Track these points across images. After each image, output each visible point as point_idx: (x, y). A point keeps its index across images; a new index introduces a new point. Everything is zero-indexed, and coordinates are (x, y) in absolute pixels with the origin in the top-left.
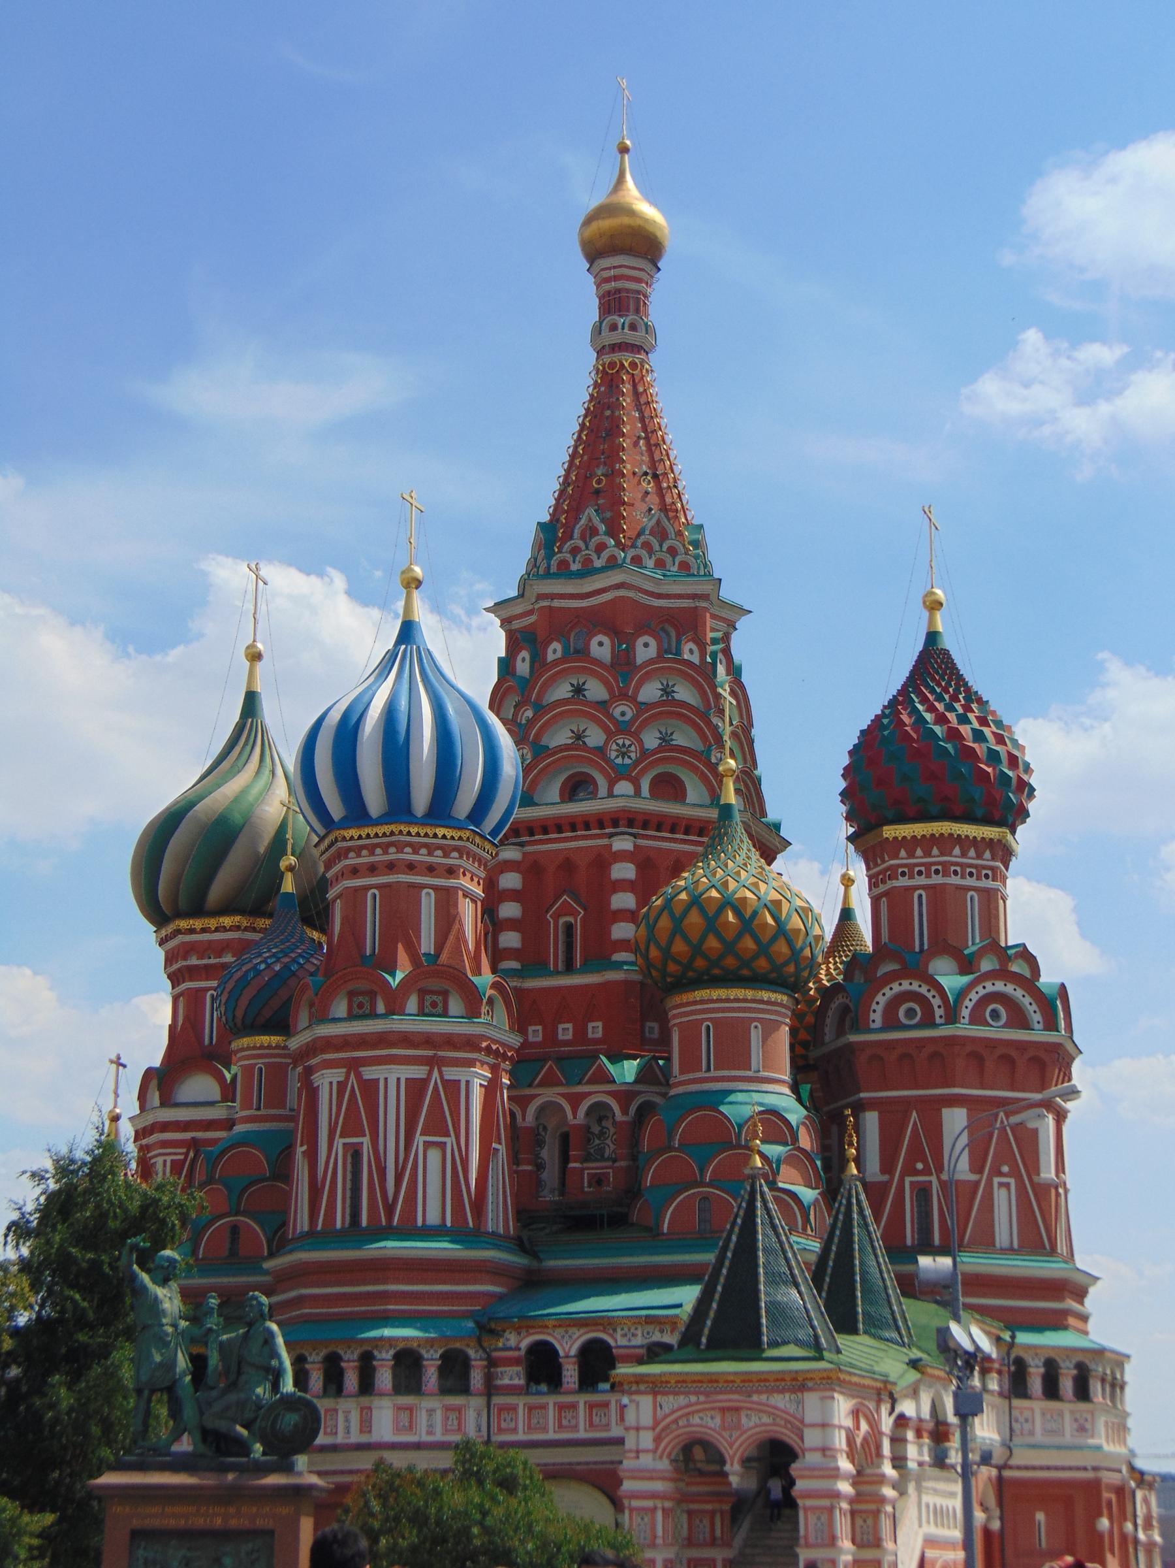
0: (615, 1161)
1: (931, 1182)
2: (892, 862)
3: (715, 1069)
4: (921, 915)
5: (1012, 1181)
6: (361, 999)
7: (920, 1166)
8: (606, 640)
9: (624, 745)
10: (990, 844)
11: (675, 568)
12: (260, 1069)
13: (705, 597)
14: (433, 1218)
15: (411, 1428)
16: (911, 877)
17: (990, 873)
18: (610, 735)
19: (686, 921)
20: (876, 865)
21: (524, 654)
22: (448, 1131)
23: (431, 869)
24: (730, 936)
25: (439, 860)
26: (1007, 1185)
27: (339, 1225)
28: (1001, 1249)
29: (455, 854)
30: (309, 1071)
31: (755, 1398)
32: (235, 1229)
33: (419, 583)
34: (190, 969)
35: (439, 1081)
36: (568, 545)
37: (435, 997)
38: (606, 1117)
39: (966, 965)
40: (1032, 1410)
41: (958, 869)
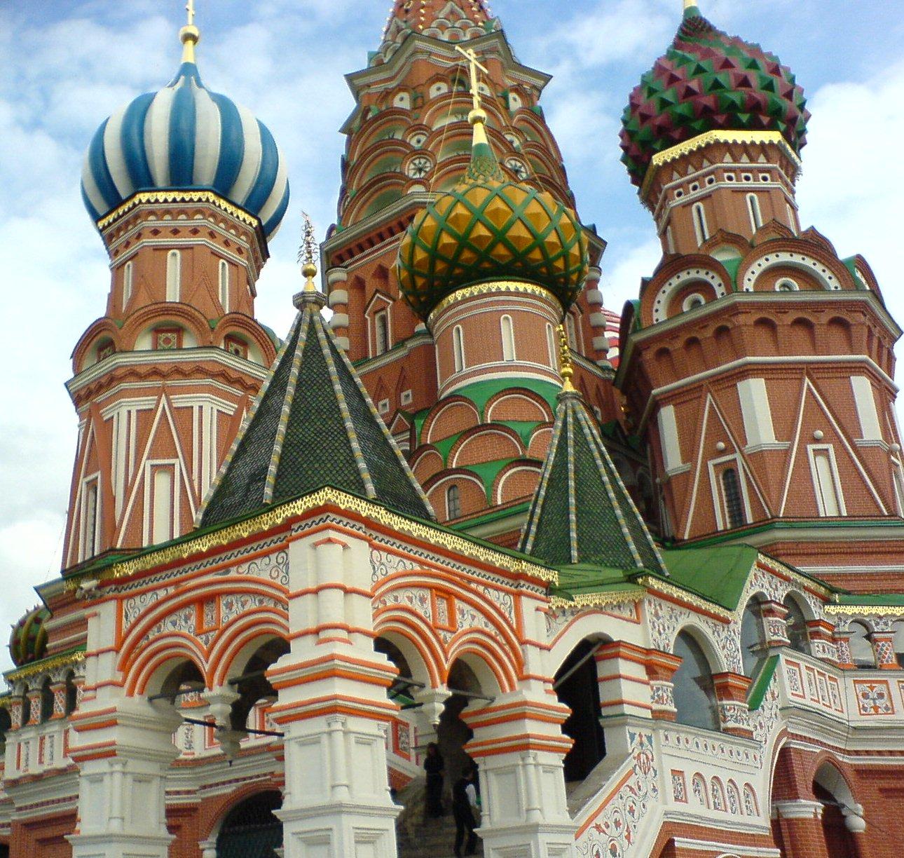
1: (735, 460)
2: (666, 186)
5: (830, 447)
7: (721, 445)
9: (420, 163)
10: (763, 148)
11: (468, 37)
16: (687, 192)
24: (461, 232)
28: (826, 517)
31: (233, 573)
40: (886, 682)
41: (733, 175)
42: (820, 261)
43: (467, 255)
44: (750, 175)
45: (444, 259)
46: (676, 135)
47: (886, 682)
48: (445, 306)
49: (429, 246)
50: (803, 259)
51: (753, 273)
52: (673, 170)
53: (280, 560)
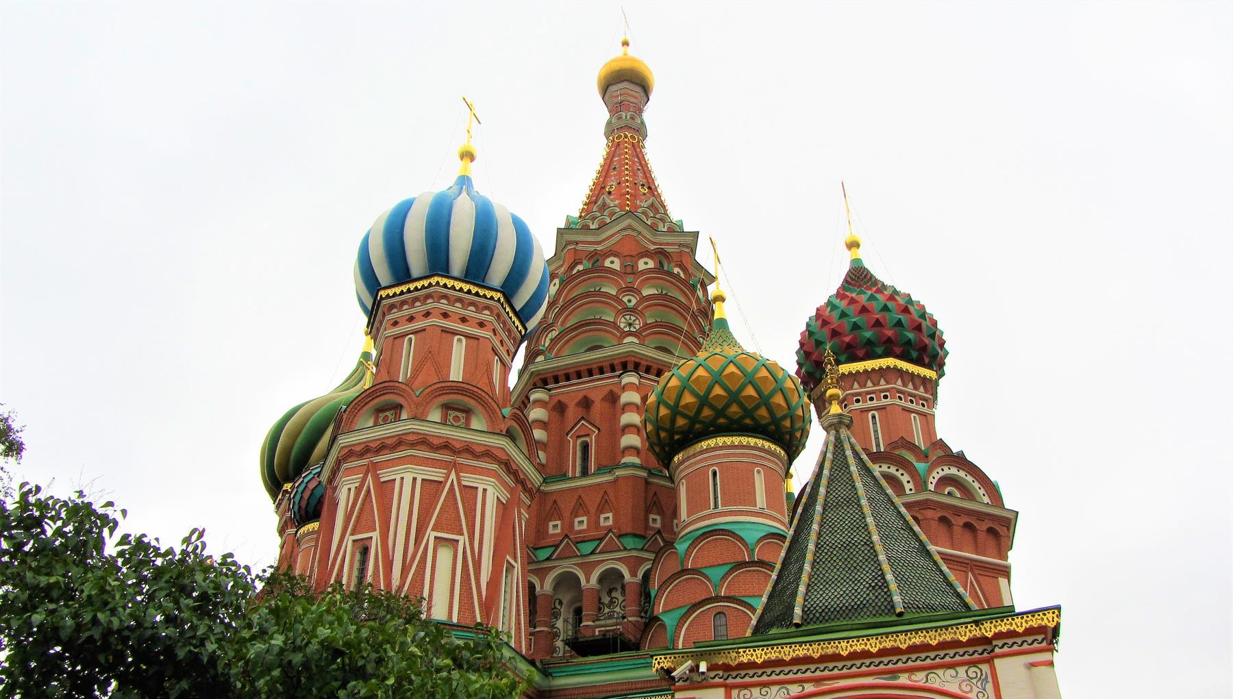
0: (624, 618)
2: (848, 392)
4: (875, 431)
8: (616, 260)
9: (630, 319)
10: (925, 381)
13: (687, 246)
16: (865, 401)
17: (925, 403)
18: (618, 312)
19: (693, 377)
21: (557, 281)
22: (462, 529)
23: (464, 320)
24: (734, 388)
25: (474, 315)
29: (487, 312)
31: (903, 679)
33: (472, 158)
35: (455, 483)
38: (615, 589)
39: (924, 457)
41: (902, 396)
42: (977, 480)
43: (734, 408)
44: (913, 399)
45: (712, 407)
46: (861, 353)
48: (705, 447)
49: (702, 394)
50: (966, 475)
51: (934, 478)
52: (855, 380)
53: (972, 675)
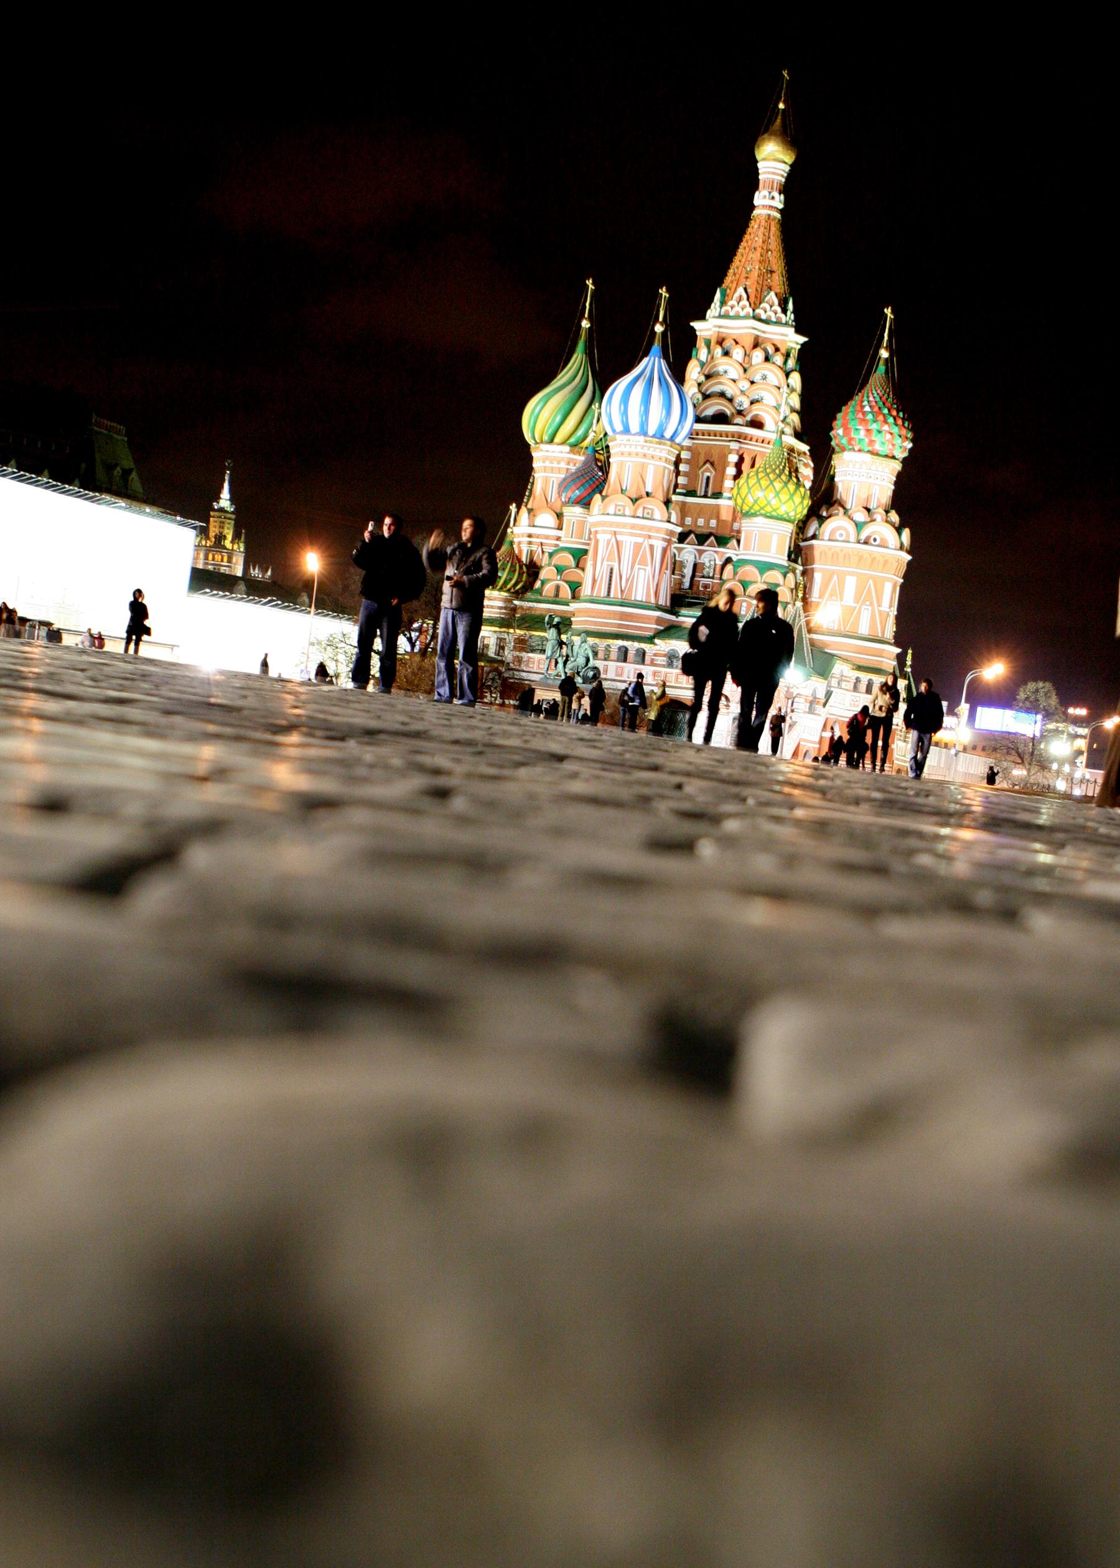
3: (757, 551)
5: (870, 608)
6: (620, 507)
7: (834, 598)
12: (574, 522)
14: (639, 598)
15: (621, 675)
20: (840, 468)
26: (868, 609)
27: (602, 596)
29: (663, 451)
30: (596, 532)
32: (558, 588)
34: (545, 467)
36: (730, 303)
37: (649, 511)
47: (860, 697)
